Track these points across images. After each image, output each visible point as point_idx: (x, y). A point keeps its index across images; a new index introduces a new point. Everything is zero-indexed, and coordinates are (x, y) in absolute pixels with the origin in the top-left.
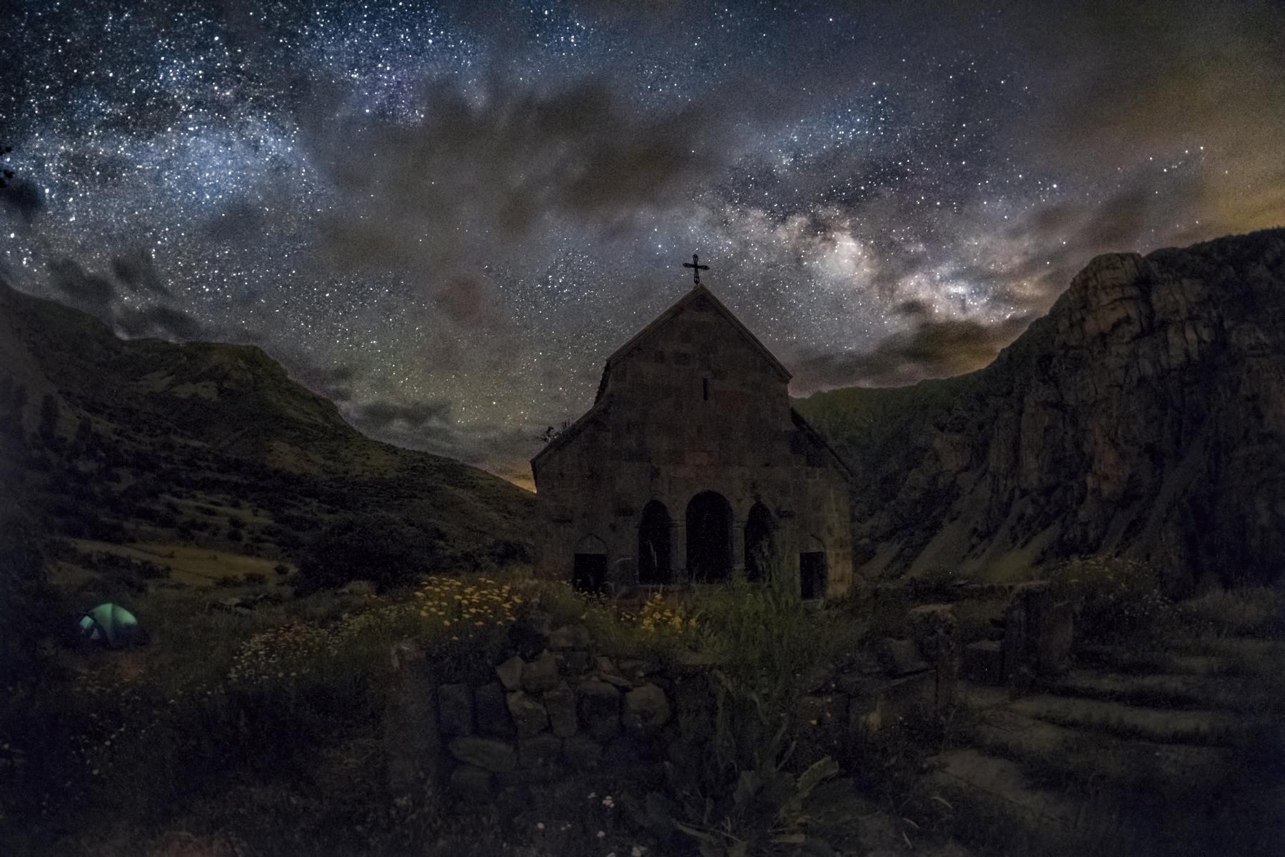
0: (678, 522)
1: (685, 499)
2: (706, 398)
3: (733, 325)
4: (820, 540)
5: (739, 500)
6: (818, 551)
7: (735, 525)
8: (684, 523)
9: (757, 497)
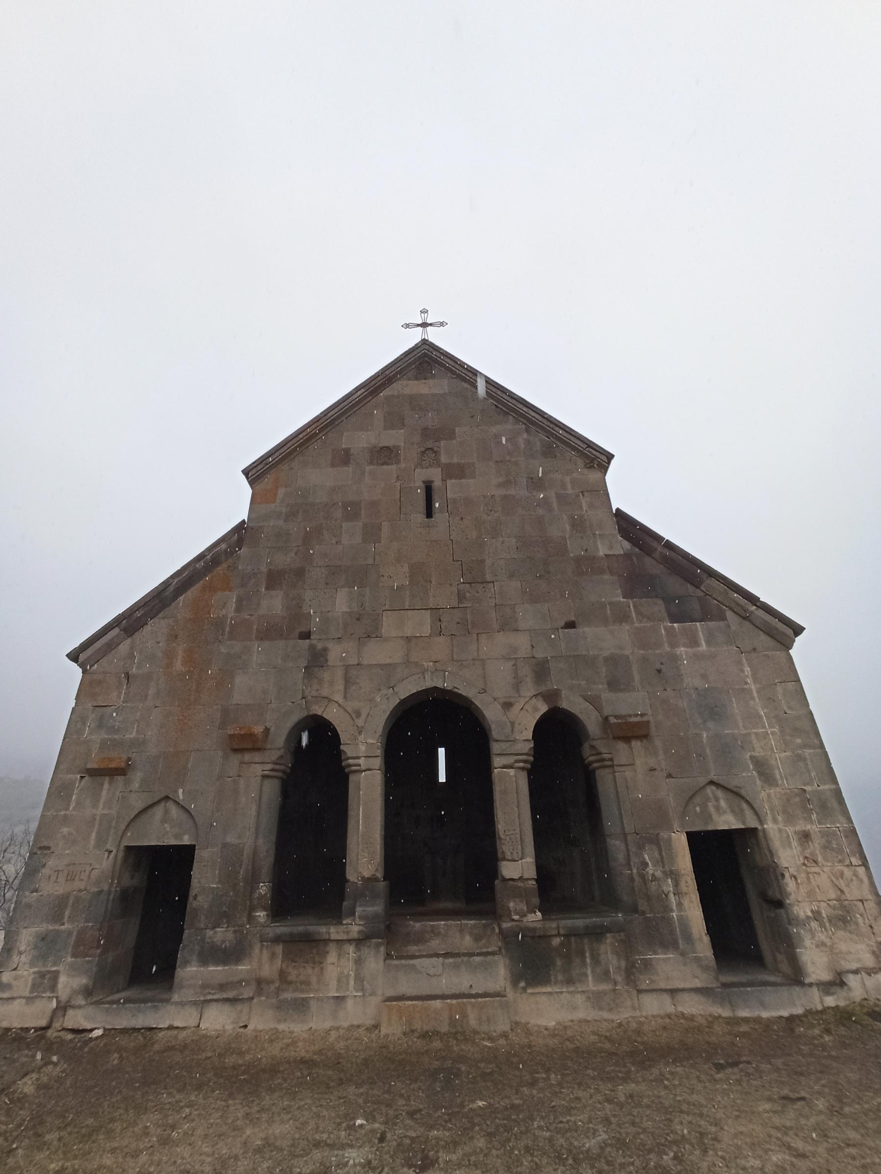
0: (361, 761)
2: (429, 513)
4: (735, 793)
5: (507, 706)
6: (736, 825)
7: (497, 761)
8: (377, 763)
9: (550, 696)
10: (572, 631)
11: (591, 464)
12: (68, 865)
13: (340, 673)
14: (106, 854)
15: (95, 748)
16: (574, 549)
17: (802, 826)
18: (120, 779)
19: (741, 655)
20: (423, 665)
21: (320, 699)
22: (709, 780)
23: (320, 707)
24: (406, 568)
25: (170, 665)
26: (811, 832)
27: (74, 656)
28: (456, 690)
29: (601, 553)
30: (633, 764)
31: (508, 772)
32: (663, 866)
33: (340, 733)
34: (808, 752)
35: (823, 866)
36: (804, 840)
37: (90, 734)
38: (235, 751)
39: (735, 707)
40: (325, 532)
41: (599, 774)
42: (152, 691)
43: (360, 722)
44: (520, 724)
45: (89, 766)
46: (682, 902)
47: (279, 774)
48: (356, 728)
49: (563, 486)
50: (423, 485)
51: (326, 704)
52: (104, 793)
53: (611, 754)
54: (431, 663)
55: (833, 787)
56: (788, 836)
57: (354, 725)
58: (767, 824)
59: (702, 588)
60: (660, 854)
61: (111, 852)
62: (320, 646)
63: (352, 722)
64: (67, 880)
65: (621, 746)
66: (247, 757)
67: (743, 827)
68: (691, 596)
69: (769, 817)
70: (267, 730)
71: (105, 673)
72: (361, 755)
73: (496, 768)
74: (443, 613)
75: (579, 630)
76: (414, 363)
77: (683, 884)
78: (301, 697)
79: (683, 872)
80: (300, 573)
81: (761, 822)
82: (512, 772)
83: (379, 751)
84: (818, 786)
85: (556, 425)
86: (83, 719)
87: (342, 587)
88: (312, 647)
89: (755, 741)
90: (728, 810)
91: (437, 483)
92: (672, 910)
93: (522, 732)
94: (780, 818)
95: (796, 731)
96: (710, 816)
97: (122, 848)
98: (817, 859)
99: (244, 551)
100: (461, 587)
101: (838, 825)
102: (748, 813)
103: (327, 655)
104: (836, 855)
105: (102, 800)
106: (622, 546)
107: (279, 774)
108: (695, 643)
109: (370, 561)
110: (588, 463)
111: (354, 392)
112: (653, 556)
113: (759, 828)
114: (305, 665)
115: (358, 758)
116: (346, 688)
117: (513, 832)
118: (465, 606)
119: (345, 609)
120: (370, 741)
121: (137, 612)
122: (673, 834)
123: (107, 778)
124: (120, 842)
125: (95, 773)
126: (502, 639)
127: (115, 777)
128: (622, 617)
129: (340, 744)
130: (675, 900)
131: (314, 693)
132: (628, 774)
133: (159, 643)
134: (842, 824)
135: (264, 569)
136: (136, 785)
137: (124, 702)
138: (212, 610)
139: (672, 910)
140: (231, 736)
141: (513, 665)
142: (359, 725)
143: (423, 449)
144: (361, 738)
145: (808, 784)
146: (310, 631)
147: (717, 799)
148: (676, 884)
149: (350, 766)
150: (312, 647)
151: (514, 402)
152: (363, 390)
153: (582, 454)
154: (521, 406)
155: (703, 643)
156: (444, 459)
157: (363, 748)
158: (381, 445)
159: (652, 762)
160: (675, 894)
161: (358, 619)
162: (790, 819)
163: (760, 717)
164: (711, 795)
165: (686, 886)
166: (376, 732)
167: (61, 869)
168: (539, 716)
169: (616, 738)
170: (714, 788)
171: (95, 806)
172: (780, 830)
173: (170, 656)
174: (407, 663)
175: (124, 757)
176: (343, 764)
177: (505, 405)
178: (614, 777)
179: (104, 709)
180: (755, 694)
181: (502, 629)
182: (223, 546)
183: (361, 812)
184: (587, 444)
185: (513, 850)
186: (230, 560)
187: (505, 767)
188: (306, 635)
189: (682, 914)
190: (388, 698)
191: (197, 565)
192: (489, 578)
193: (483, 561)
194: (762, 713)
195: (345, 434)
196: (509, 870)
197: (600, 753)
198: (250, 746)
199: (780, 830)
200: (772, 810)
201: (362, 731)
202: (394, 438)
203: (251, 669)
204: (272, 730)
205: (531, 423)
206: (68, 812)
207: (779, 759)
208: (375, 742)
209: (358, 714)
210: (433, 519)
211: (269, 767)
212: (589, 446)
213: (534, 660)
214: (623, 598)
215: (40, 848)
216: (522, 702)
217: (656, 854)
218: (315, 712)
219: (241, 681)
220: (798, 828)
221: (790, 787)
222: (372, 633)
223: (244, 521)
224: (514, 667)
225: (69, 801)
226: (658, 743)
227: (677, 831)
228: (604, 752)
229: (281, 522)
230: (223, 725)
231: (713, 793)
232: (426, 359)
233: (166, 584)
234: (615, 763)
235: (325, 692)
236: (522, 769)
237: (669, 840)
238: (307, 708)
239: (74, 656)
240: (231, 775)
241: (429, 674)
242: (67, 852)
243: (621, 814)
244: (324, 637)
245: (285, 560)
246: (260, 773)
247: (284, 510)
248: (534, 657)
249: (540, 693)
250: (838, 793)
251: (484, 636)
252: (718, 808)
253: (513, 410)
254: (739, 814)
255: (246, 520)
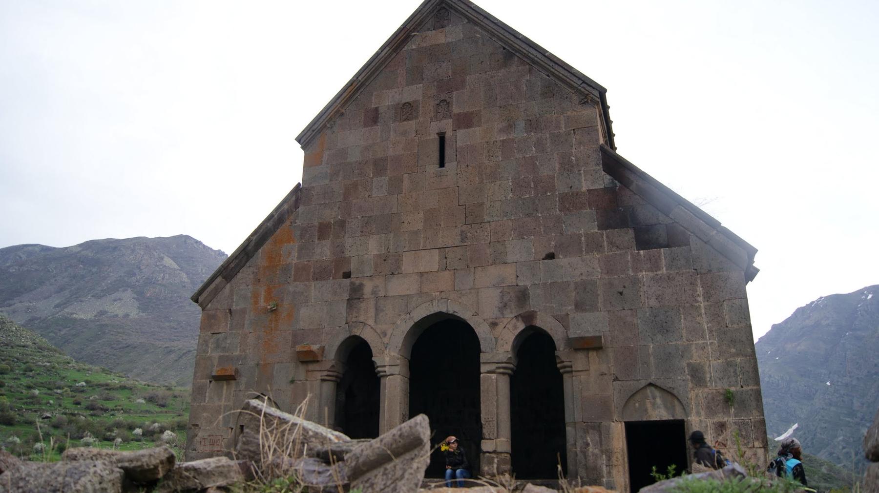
0: (386, 369)
1: (404, 326)
2: (442, 164)
3: (493, 35)
4: (668, 393)
5: (494, 325)
7: (484, 368)
9: (528, 317)
10: (550, 261)
11: (586, 100)
12: (209, 436)
13: (372, 302)
14: (230, 430)
15: (216, 363)
16: (561, 187)
17: (720, 418)
18: (233, 382)
19: (697, 276)
20: (432, 295)
21: (358, 323)
22: (648, 382)
23: (358, 329)
24: (421, 215)
25: (256, 303)
26: (727, 423)
27: (196, 299)
28: (456, 314)
29: (584, 189)
30: (587, 370)
31: (491, 377)
32: (601, 445)
33: (372, 348)
34: (738, 360)
35: (730, 448)
36: (719, 428)
37: (211, 352)
38: (303, 362)
39: (683, 323)
40: (360, 188)
41: (565, 376)
42: (247, 322)
43: (386, 340)
44: (502, 339)
45: (214, 374)
46: (611, 471)
47: (334, 378)
48: (382, 344)
49: (558, 127)
50: (437, 137)
51: (362, 327)
52: (224, 392)
53: (571, 362)
54: (438, 293)
55: (755, 388)
56: (707, 426)
57: (381, 343)
58: (691, 417)
59: (671, 216)
60: (600, 437)
61: (232, 429)
62: (357, 282)
63: (380, 340)
64: (210, 445)
65: (581, 356)
66: (311, 367)
67: (672, 418)
68: (660, 224)
69: (694, 411)
70: (323, 349)
71: (217, 309)
72: (386, 364)
73: (482, 373)
74: (448, 252)
75: (556, 261)
76: (433, 12)
77: (614, 459)
78: (345, 322)
79: (615, 450)
80: (342, 224)
81: (687, 415)
82: (494, 376)
83: (399, 361)
84: (742, 387)
85: (556, 63)
86: (206, 342)
87: (373, 234)
88: (352, 284)
89: (694, 351)
90: (662, 406)
91: (449, 135)
92: (603, 477)
93: (503, 346)
94: (703, 413)
95: (733, 341)
96: (646, 410)
97: (239, 426)
98: (727, 443)
99: (301, 209)
100: (464, 228)
101: (751, 418)
102: (678, 408)
103: (363, 290)
104: (743, 440)
105: (224, 396)
106: (604, 180)
107: (334, 378)
108: (656, 267)
109: (394, 211)
110: (583, 99)
111: (380, 51)
112: (631, 188)
113: (685, 419)
114: (347, 298)
115: (384, 366)
116: (376, 315)
117: (491, 420)
118: (465, 244)
119: (376, 252)
120: (392, 354)
121: (232, 264)
122: (612, 423)
123: (225, 382)
124: (237, 423)
125: (218, 378)
126: (494, 272)
127: (230, 381)
128: (594, 245)
129: (371, 356)
130: (606, 470)
131: (354, 320)
132: (583, 377)
133: (248, 286)
134: (755, 417)
135: (316, 223)
136: (242, 387)
137: (230, 330)
138: (282, 258)
139: (603, 477)
140: (299, 352)
141: (500, 293)
142: (386, 343)
143: (437, 102)
144: (386, 352)
145: (733, 386)
146: (350, 272)
147: (654, 398)
148: (609, 459)
149: (379, 372)
150: (352, 284)
151: (519, 42)
152: (388, 48)
153: (578, 91)
154: (524, 46)
155: (664, 269)
156: (456, 110)
157: (387, 359)
158: (403, 102)
159: (604, 368)
160: (607, 466)
161: (385, 260)
162: (711, 411)
163: (704, 331)
164: (650, 394)
165: (617, 461)
166: (397, 347)
167: (206, 438)
168: (518, 333)
169: (577, 350)
170: (653, 388)
171: (220, 400)
172: (701, 421)
173: (256, 296)
174: (420, 293)
175: (234, 368)
176: (376, 371)
177: (511, 46)
178: (572, 379)
179: (218, 335)
180: (703, 311)
181: (494, 263)
182: (286, 207)
183: (386, 404)
184: (582, 80)
185: (490, 432)
186: (292, 217)
187: (489, 372)
188: (347, 275)
189: (610, 479)
190: (405, 322)
191: (268, 224)
192: (486, 218)
193: (482, 204)
194: (706, 327)
195: (374, 93)
196: (487, 446)
197: (563, 362)
198: (311, 359)
199: (701, 421)
200: (698, 405)
201: (387, 347)
202: (413, 93)
203: (311, 303)
204: (326, 347)
205: (534, 63)
206: (205, 404)
207: (712, 365)
208: (396, 354)
209: (385, 335)
210: (443, 168)
211: (326, 373)
212: (584, 82)
213: (517, 287)
214: (598, 230)
215: (193, 425)
216: (505, 321)
217: (597, 438)
218: (355, 334)
219: (304, 312)
220: (716, 420)
221: (716, 388)
222: (395, 272)
223: (299, 184)
224: (501, 294)
225: (205, 397)
226: (611, 355)
227: (616, 421)
228: (565, 360)
229: (327, 182)
230: (295, 343)
231: (651, 392)
232: (444, 5)
233: (249, 240)
234: (574, 369)
235: (362, 319)
236: (503, 374)
237: (608, 429)
238: (350, 332)
239: (196, 299)
240: (301, 379)
241: (436, 301)
242: (208, 428)
243: (574, 408)
244: (360, 275)
245: (331, 215)
246: (320, 378)
247: (329, 171)
248: (517, 285)
249: (520, 314)
250: (758, 395)
251: (480, 269)
252: (654, 404)
253: (518, 51)
254: (669, 408)
255: (301, 183)
